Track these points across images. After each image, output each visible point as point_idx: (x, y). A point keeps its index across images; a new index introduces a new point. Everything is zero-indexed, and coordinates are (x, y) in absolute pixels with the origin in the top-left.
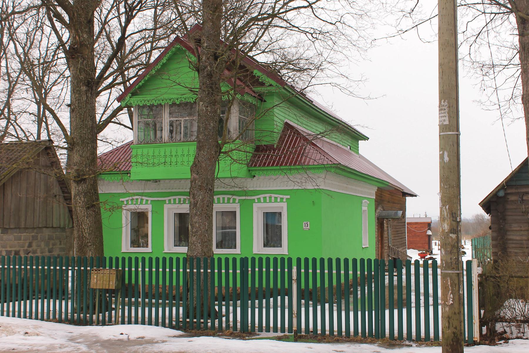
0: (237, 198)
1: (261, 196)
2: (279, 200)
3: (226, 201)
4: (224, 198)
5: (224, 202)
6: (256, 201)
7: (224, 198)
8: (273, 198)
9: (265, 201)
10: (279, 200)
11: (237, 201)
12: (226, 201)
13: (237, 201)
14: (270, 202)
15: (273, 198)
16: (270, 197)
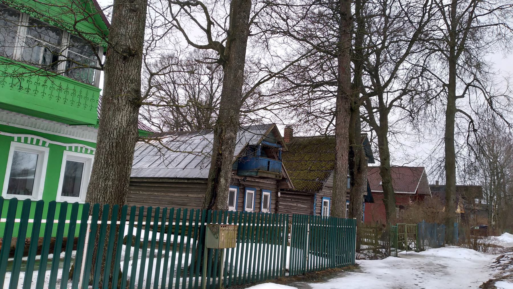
0: (48, 142)
1: (74, 145)
2: (89, 152)
3: (35, 142)
4: (32, 139)
5: (32, 143)
6: (68, 149)
7: (32, 139)
8: (84, 149)
9: (76, 151)
10: (89, 152)
11: (47, 145)
12: (35, 142)
13: (47, 145)
14: (81, 152)
15: (84, 149)
16: (82, 148)
